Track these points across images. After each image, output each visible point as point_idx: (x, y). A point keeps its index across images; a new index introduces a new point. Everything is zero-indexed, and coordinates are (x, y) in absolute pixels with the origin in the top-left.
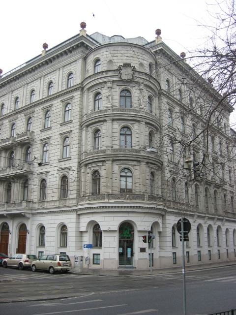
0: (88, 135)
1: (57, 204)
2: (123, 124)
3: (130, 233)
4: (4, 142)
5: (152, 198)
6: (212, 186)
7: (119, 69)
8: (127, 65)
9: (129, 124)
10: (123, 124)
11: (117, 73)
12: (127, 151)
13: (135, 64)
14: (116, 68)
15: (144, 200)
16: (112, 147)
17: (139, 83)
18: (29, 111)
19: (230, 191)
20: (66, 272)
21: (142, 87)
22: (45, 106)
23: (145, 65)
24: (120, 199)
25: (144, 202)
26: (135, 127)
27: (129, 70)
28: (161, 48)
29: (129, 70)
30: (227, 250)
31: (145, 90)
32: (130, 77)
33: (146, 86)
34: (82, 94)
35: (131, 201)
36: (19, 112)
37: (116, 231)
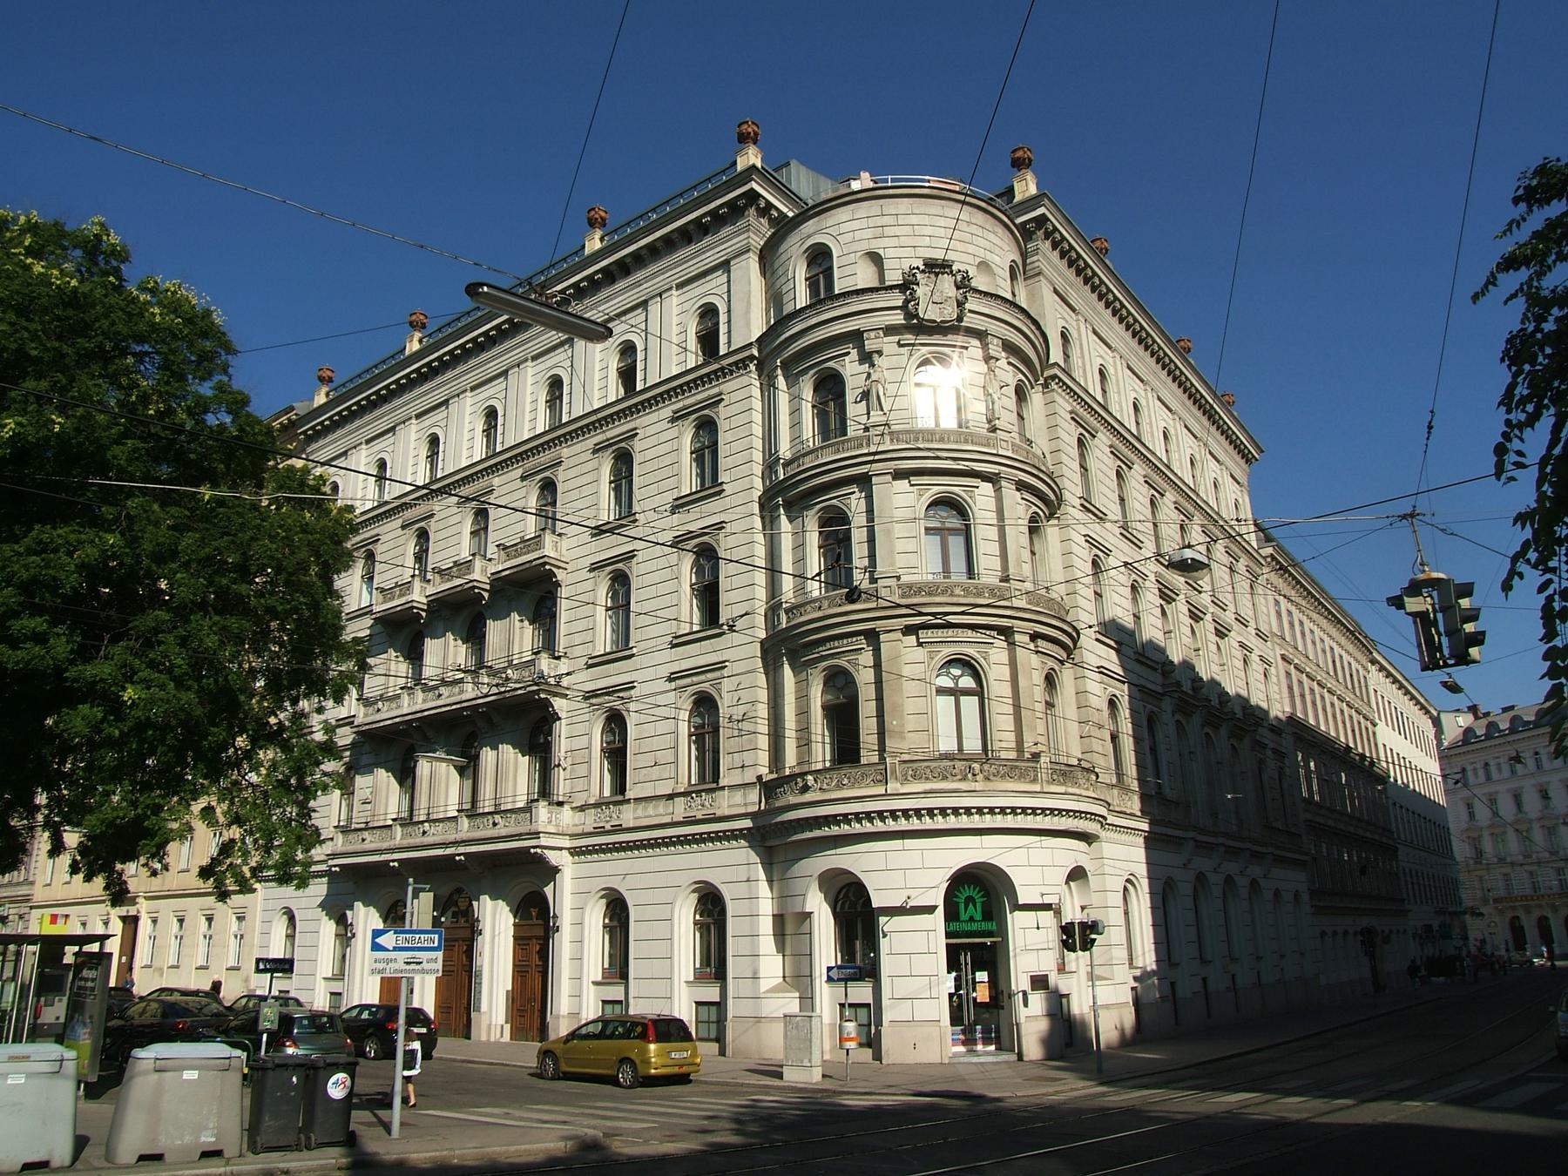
0: (802, 542)
1: (679, 809)
2: (937, 487)
3: (988, 915)
4: (509, 557)
5: (1064, 774)
6: (1223, 731)
7: (907, 285)
8: (936, 267)
9: (955, 487)
10: (937, 487)
11: (897, 299)
12: (958, 591)
13: (962, 261)
14: (893, 277)
15: (1034, 781)
16: (898, 578)
17: (981, 335)
18: (545, 458)
19: (1275, 751)
20: (682, 1079)
21: (995, 349)
22: (610, 434)
23: (997, 270)
24: (945, 778)
25: (1037, 788)
26: (981, 499)
27: (946, 284)
28: (1041, 211)
29: (946, 284)
30: (1204, 980)
31: (1003, 363)
32: (950, 313)
33: (1009, 347)
34: (768, 386)
35: (990, 786)
36: (445, 491)
37: (930, 909)
